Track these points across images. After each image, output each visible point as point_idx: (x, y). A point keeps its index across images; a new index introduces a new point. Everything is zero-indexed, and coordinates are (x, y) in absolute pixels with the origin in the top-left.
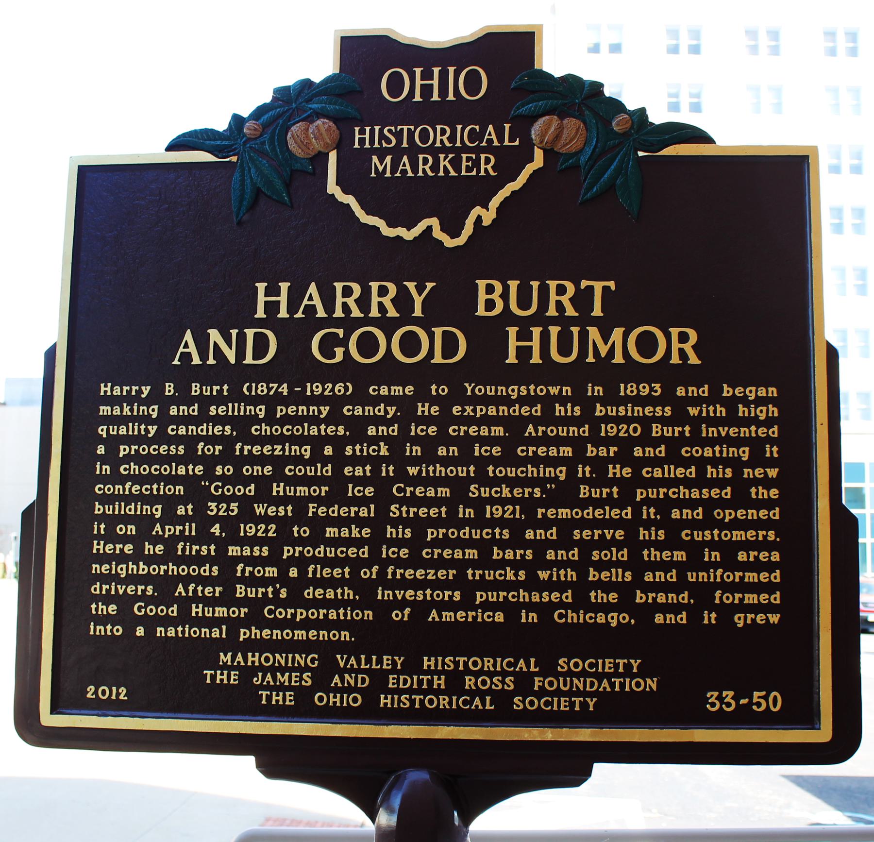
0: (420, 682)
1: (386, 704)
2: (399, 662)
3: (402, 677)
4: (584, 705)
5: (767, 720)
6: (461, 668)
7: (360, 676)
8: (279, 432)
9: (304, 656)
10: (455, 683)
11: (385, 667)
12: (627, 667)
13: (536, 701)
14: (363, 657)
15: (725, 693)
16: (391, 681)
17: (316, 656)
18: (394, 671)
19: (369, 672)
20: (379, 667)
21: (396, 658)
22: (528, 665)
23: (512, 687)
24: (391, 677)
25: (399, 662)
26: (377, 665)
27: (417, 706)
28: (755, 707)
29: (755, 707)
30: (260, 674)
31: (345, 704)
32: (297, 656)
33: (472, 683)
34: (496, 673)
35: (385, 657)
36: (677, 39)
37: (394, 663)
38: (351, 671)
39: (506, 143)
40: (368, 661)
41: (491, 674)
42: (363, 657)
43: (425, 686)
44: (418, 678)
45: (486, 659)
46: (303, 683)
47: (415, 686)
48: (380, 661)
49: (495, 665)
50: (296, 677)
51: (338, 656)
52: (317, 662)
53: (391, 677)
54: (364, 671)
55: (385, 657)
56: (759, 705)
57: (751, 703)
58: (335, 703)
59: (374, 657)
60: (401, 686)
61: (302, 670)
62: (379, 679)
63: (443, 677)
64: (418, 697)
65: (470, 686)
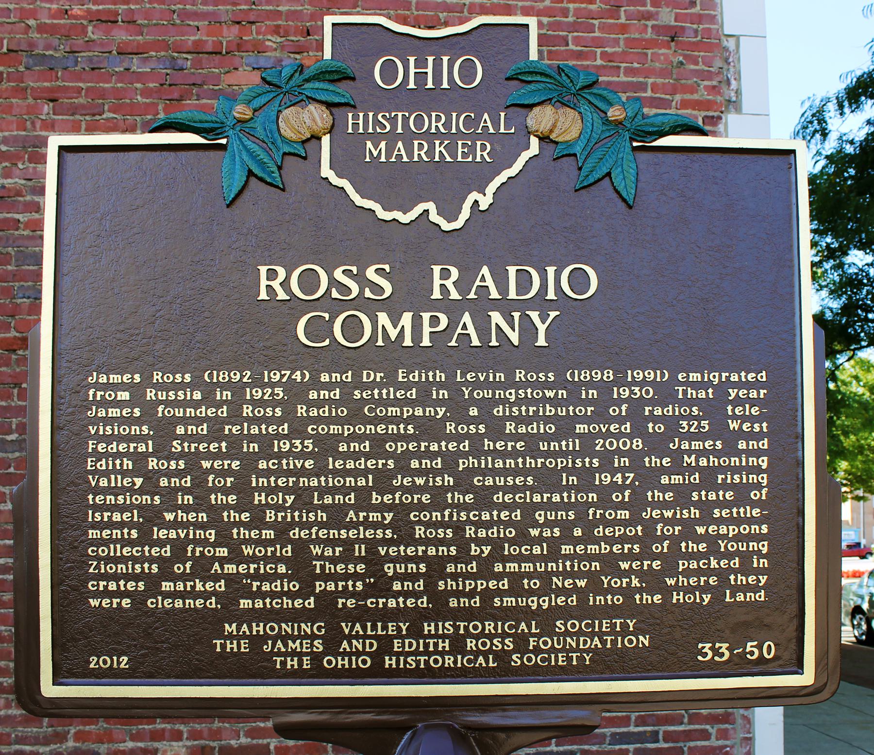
0: (426, 645)
1: (390, 665)
2: (404, 628)
3: (407, 641)
4: (581, 659)
5: (761, 667)
6: (462, 632)
7: (368, 641)
8: (518, 552)
9: (309, 624)
10: (458, 645)
11: (390, 633)
12: (624, 626)
13: (534, 658)
14: (369, 624)
15: (718, 645)
16: (396, 645)
17: (323, 624)
18: (399, 636)
19: (376, 637)
20: (384, 633)
21: (401, 624)
22: (529, 627)
23: (512, 647)
24: (395, 641)
25: (404, 628)
26: (382, 631)
27: (422, 666)
28: (748, 656)
29: (748, 656)
30: (270, 642)
31: (354, 666)
32: (303, 625)
33: (473, 645)
34: (496, 635)
35: (390, 624)
36: (863, 573)
37: (399, 629)
38: (357, 637)
39: (502, 130)
40: (374, 627)
41: (491, 637)
42: (369, 624)
43: (431, 649)
44: (424, 643)
45: (487, 623)
46: (315, 649)
47: (421, 649)
48: (385, 628)
49: (496, 628)
50: (307, 643)
51: (343, 624)
52: (323, 630)
53: (395, 641)
54: (370, 637)
55: (390, 624)
56: (752, 653)
57: (745, 653)
58: (343, 665)
59: (379, 624)
60: (407, 649)
61: (313, 637)
62: (385, 645)
63: (426, 632)
64: (422, 658)
65: (471, 647)
